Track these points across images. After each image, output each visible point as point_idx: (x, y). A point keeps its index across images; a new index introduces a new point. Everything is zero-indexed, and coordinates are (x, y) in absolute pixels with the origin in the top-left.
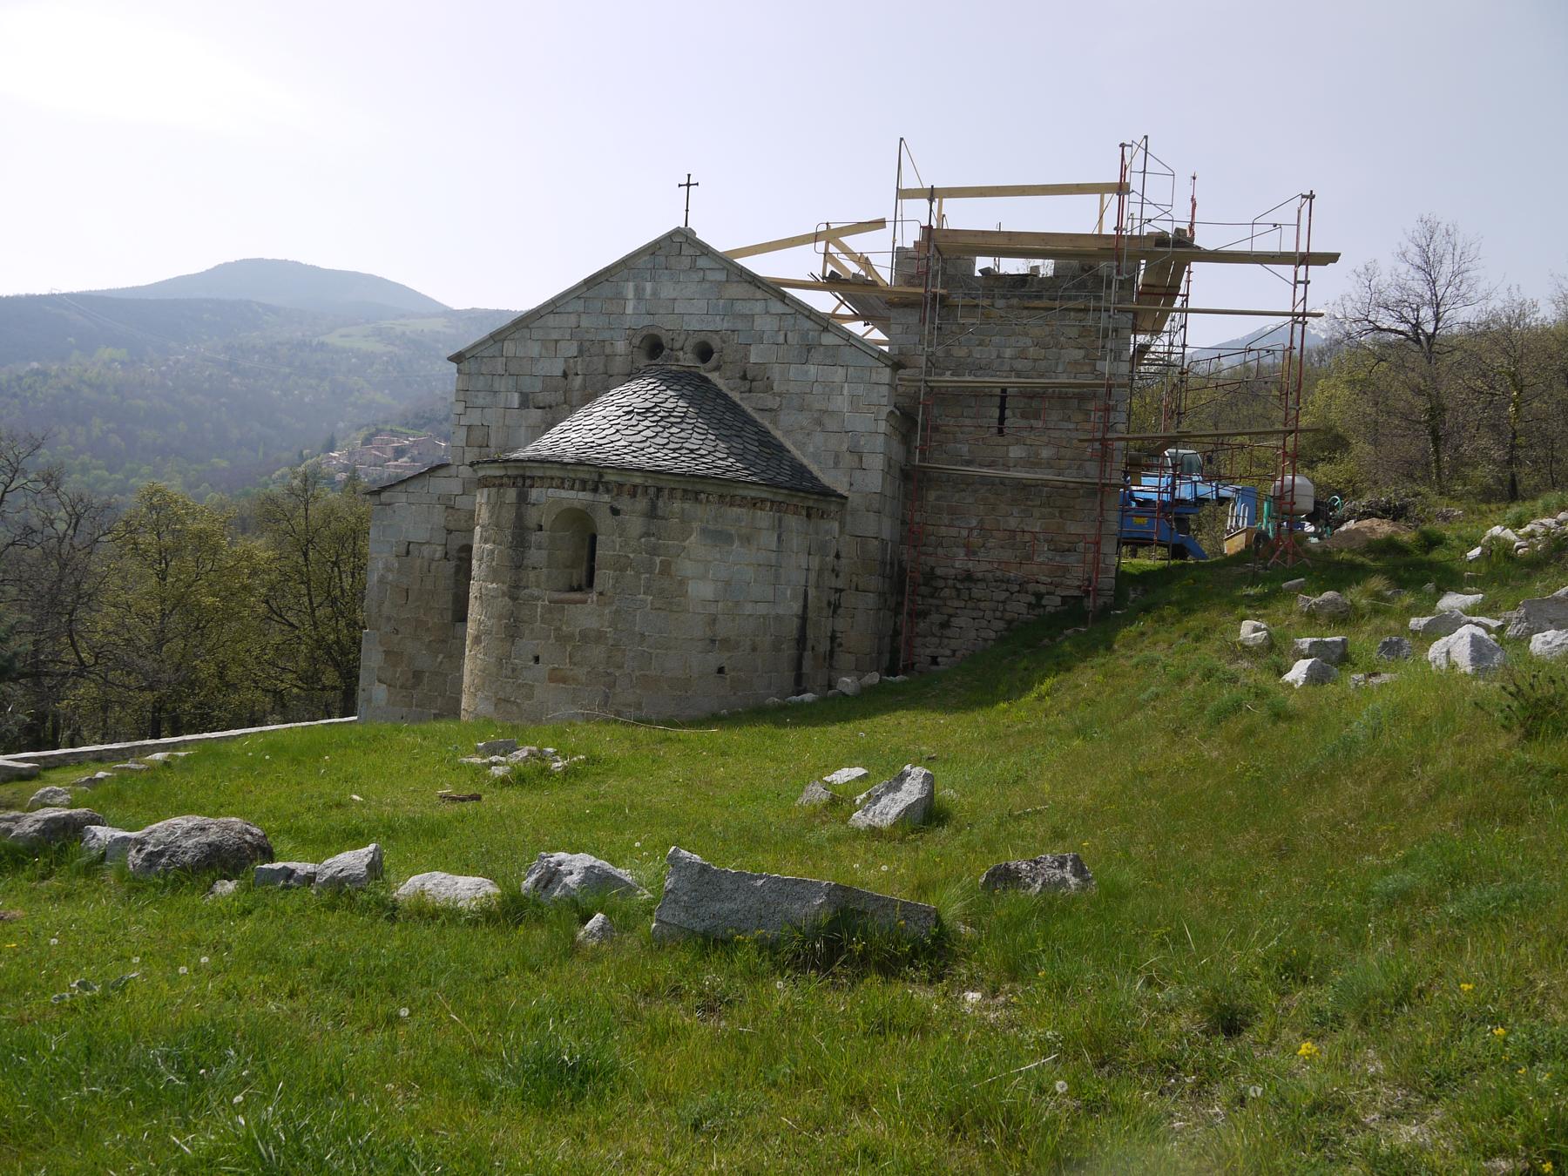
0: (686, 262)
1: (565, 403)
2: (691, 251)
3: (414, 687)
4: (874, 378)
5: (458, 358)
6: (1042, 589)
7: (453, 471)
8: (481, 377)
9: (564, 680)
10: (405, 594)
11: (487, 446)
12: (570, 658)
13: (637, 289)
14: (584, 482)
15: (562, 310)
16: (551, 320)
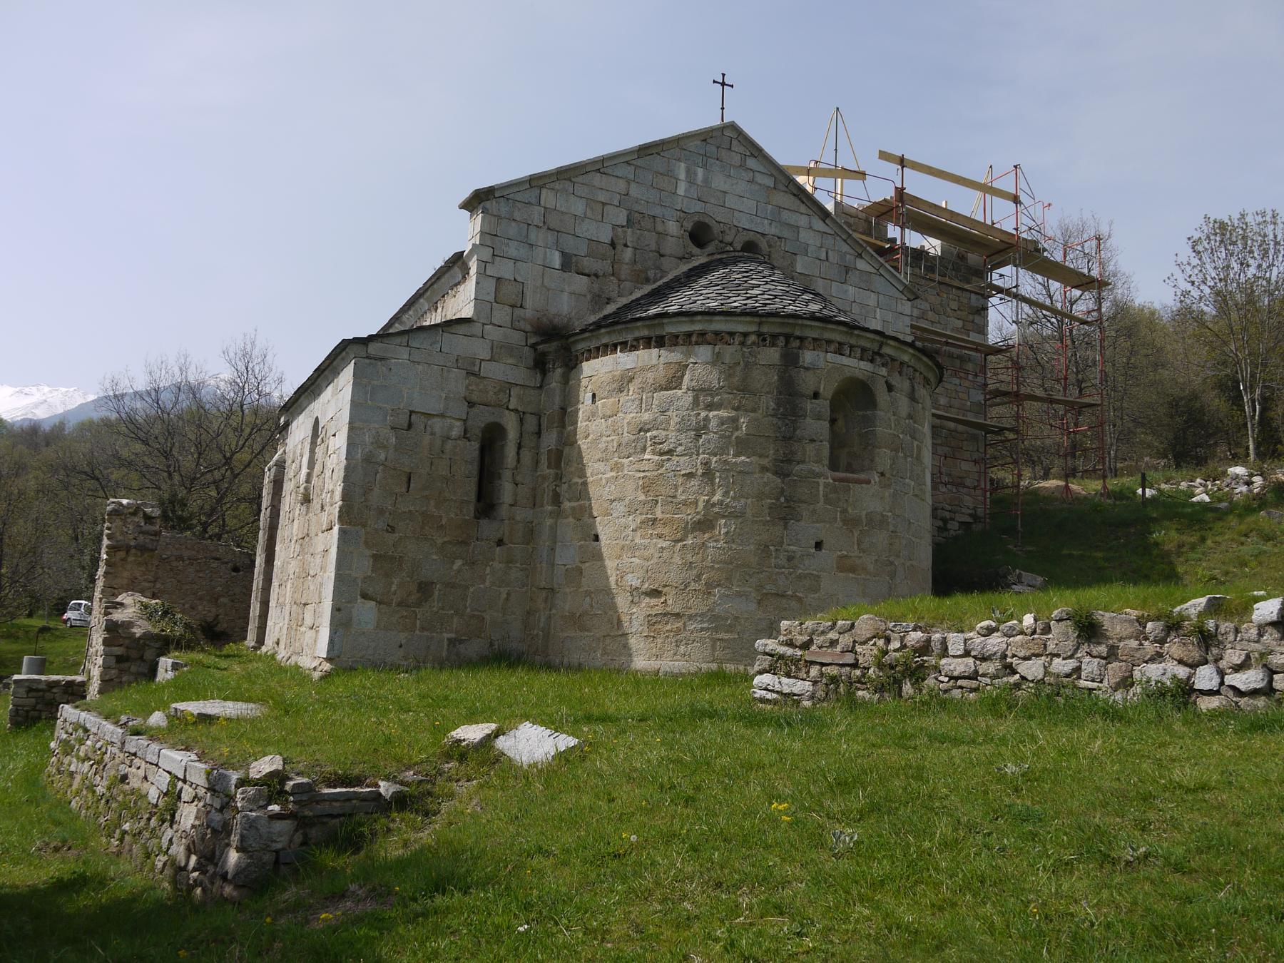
0: (737, 159)
1: (613, 275)
2: (741, 149)
3: (419, 604)
4: (900, 309)
5: (478, 201)
6: (947, 515)
7: (477, 329)
8: (513, 224)
9: (853, 569)
10: (405, 479)
11: (521, 307)
12: (858, 544)
13: (688, 171)
14: (864, 350)
15: (609, 171)
16: (597, 179)
